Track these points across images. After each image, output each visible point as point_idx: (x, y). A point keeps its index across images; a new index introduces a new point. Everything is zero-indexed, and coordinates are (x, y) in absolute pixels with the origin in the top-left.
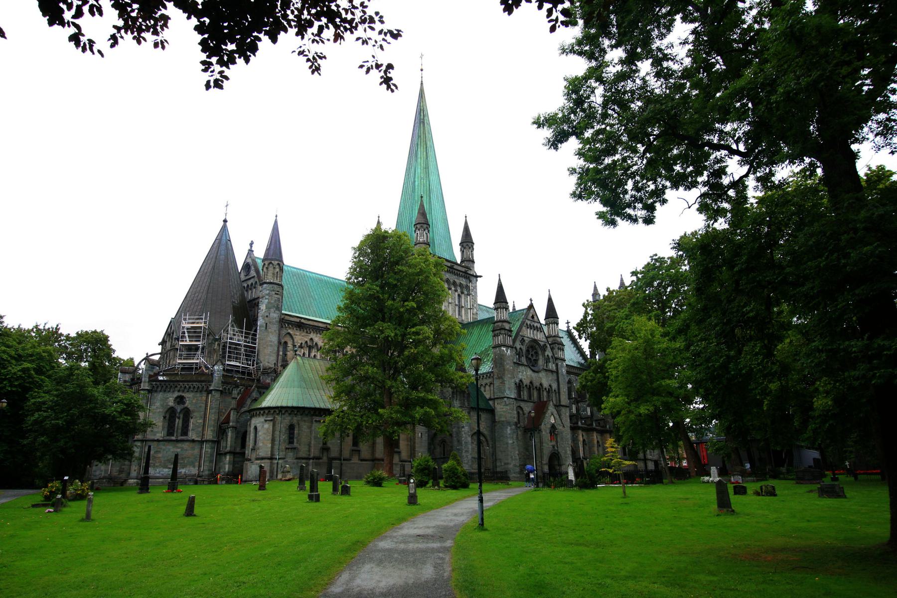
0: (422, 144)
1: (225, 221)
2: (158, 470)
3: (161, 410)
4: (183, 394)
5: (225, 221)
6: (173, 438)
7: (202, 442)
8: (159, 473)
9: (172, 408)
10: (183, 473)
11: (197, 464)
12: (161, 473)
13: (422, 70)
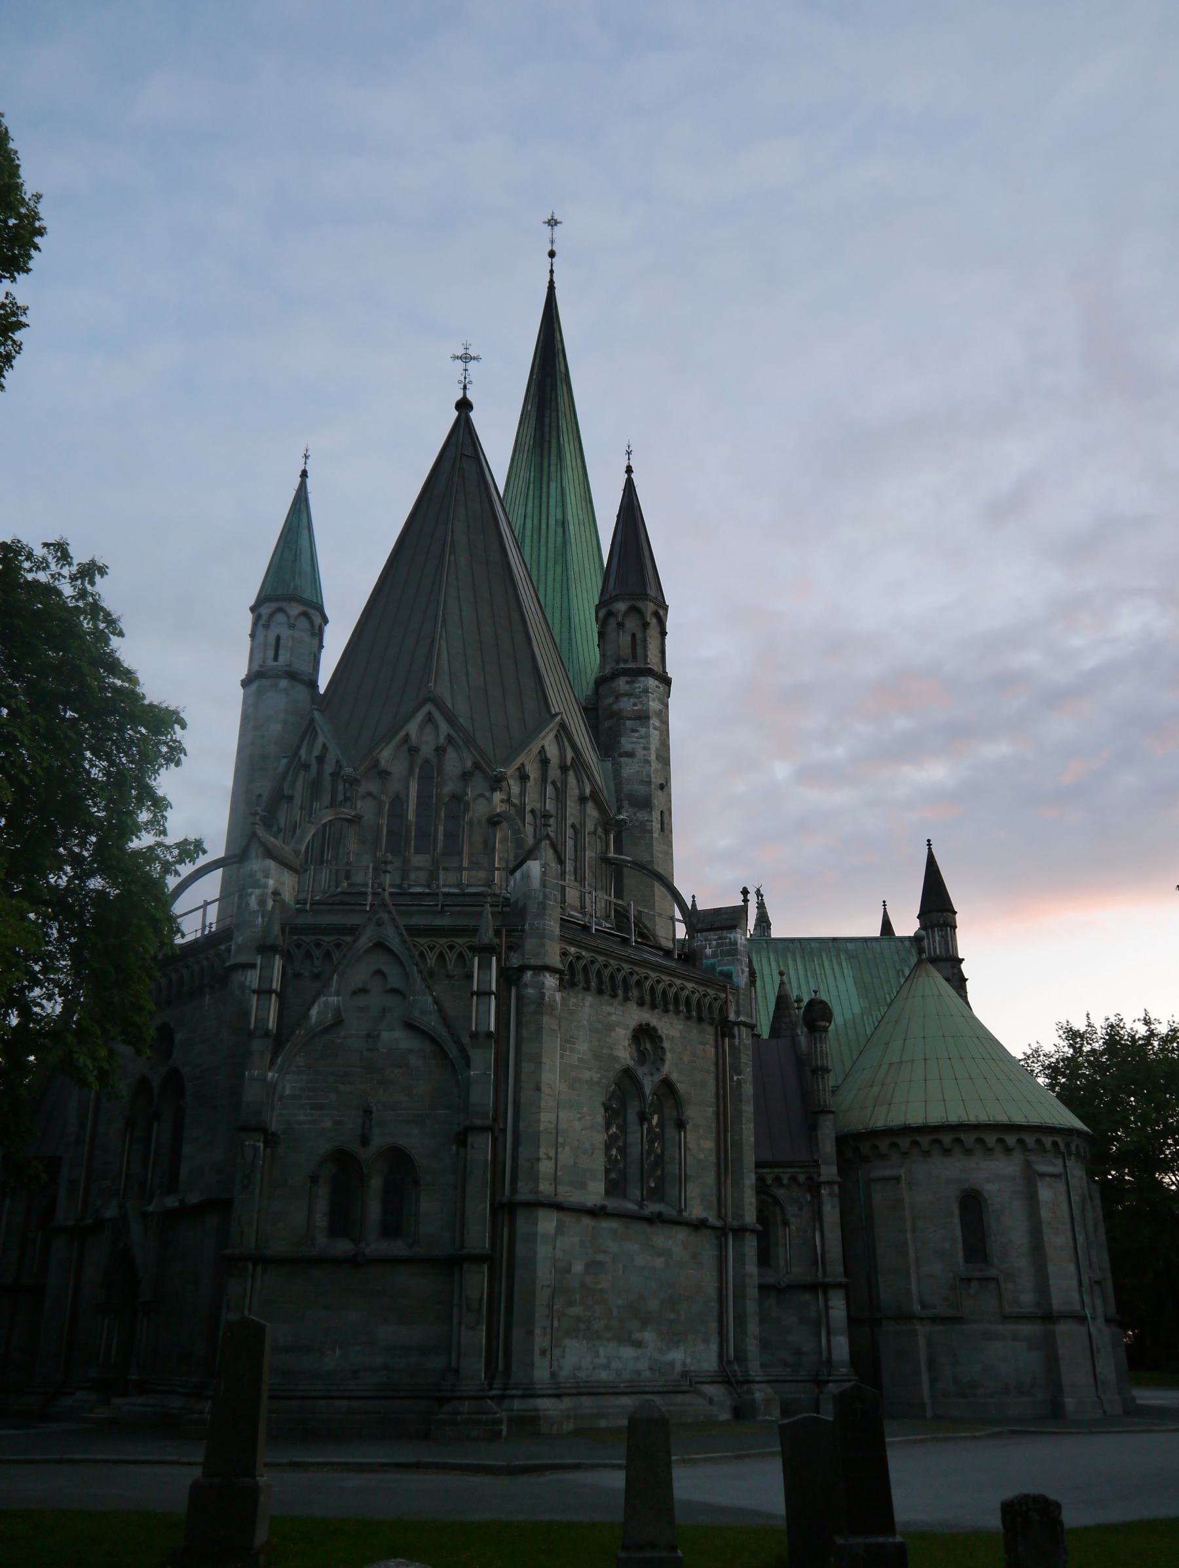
0: (571, 436)
1: (464, 406)
2: (601, 1350)
3: (596, 1076)
4: (654, 1022)
5: (464, 406)
6: (631, 1207)
7: (722, 1232)
8: (607, 1367)
9: (627, 1072)
10: (678, 1368)
11: (714, 1325)
12: (616, 1365)
13: (552, 254)
